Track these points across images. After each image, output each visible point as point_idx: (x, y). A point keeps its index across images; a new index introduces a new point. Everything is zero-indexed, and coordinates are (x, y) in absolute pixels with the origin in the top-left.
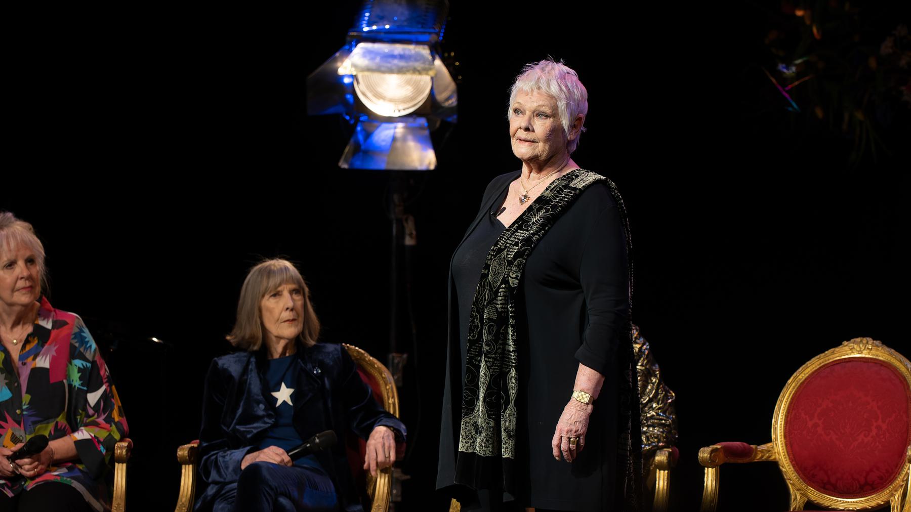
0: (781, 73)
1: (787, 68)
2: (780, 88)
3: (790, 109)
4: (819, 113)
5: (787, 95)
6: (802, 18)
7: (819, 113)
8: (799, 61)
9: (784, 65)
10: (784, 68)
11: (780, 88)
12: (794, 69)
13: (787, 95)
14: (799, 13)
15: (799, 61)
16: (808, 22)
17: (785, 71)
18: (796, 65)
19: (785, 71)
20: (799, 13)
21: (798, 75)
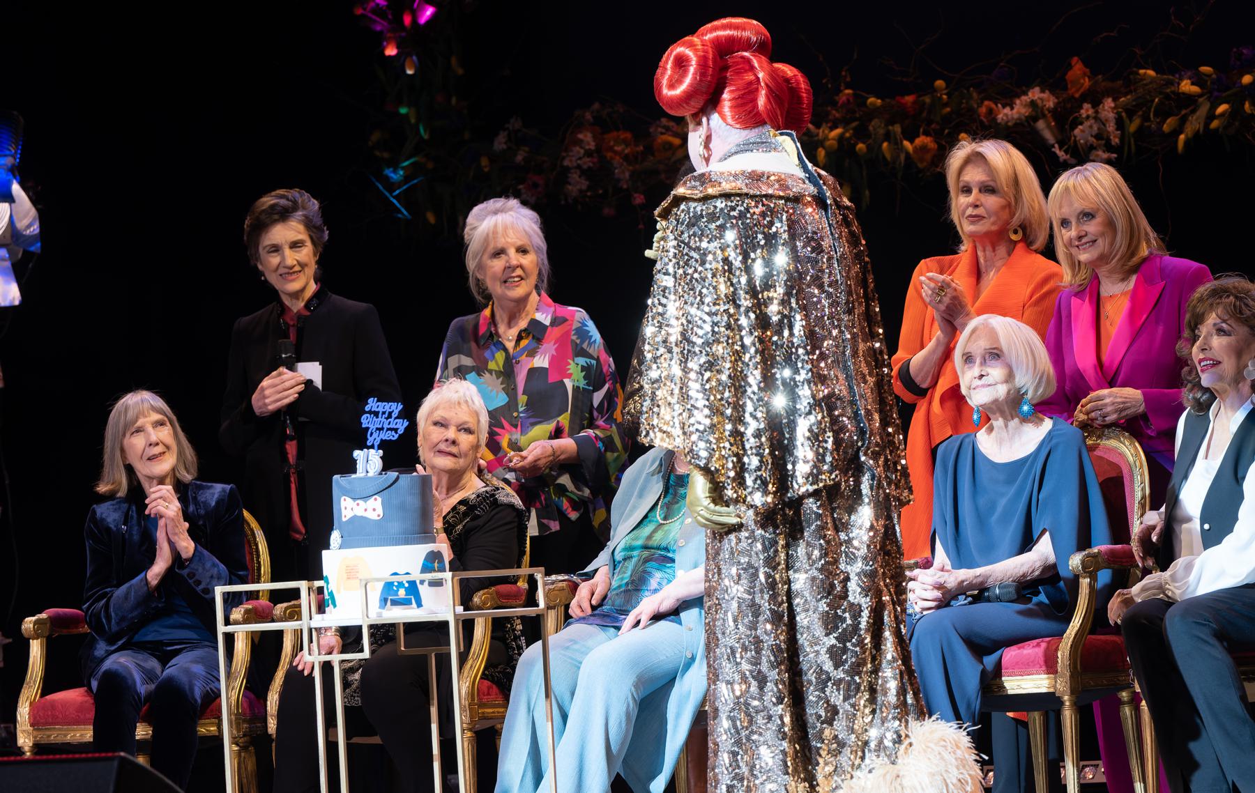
0: (387, 178)
1: (395, 172)
2: (387, 194)
3: (400, 216)
4: (431, 218)
5: (395, 201)
6: (406, 116)
7: (431, 218)
8: (406, 164)
9: (391, 169)
10: (391, 172)
11: (387, 194)
12: (401, 173)
13: (395, 201)
14: (403, 111)
15: (406, 164)
16: (413, 121)
17: (392, 175)
18: (403, 168)
19: (392, 175)
20: (403, 111)
21: (407, 179)
